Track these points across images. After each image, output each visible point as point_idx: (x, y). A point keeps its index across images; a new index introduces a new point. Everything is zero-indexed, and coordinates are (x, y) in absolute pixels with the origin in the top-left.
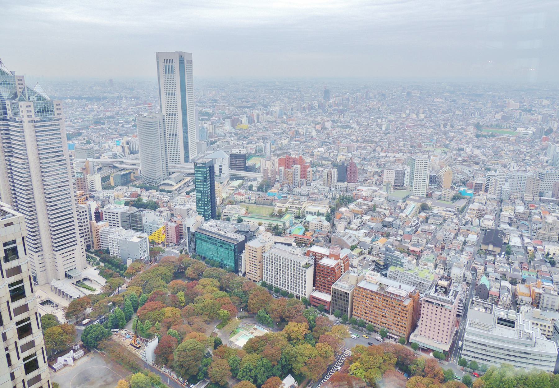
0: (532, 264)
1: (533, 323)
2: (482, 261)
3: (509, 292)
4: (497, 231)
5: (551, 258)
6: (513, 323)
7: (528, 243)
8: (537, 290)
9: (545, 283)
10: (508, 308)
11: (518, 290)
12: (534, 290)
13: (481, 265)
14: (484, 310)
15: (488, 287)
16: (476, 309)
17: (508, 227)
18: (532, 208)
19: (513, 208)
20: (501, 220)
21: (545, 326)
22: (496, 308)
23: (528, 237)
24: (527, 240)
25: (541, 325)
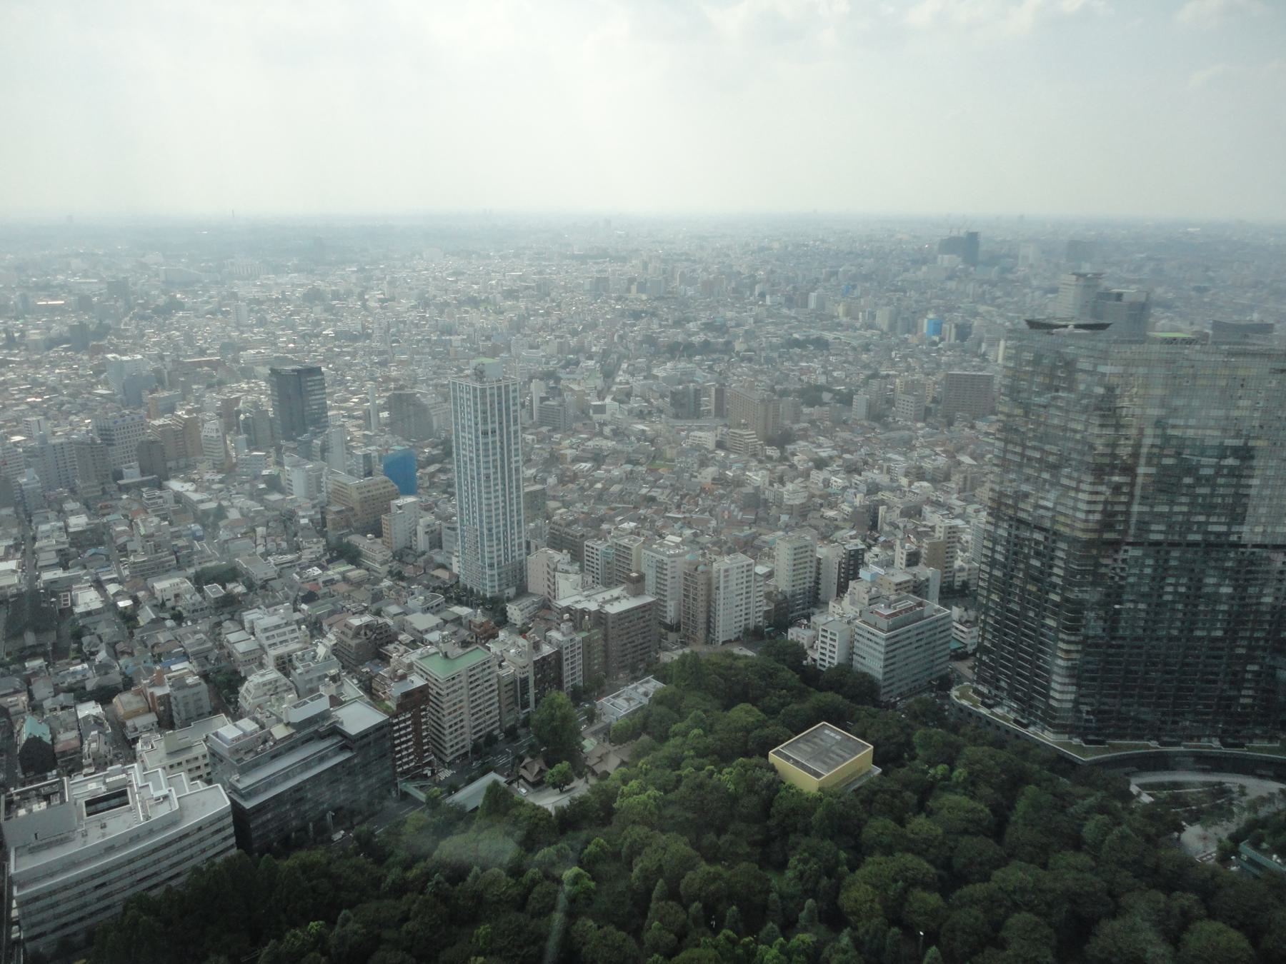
0: (137, 637)
1: (171, 767)
2: (17, 682)
3: (101, 725)
4: (34, 593)
5: (173, 608)
6: (124, 793)
7: (117, 594)
8: (159, 692)
9: (174, 668)
10: (101, 764)
11: (121, 711)
12: (152, 694)
13: (16, 692)
14: (44, 804)
15: (47, 738)
16: (22, 812)
17: (59, 573)
18: (105, 511)
19: (61, 524)
20: (40, 564)
21: (197, 759)
22: (80, 778)
23: (112, 581)
24: (112, 589)
25: (187, 761)
